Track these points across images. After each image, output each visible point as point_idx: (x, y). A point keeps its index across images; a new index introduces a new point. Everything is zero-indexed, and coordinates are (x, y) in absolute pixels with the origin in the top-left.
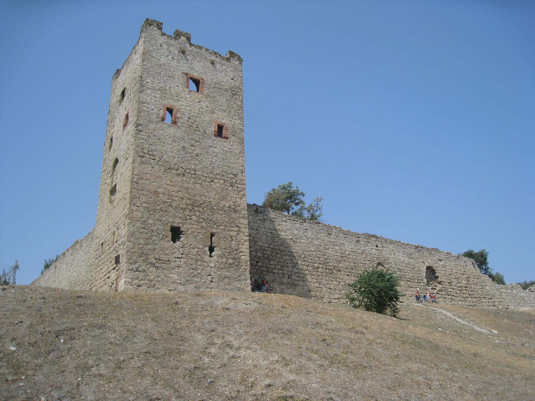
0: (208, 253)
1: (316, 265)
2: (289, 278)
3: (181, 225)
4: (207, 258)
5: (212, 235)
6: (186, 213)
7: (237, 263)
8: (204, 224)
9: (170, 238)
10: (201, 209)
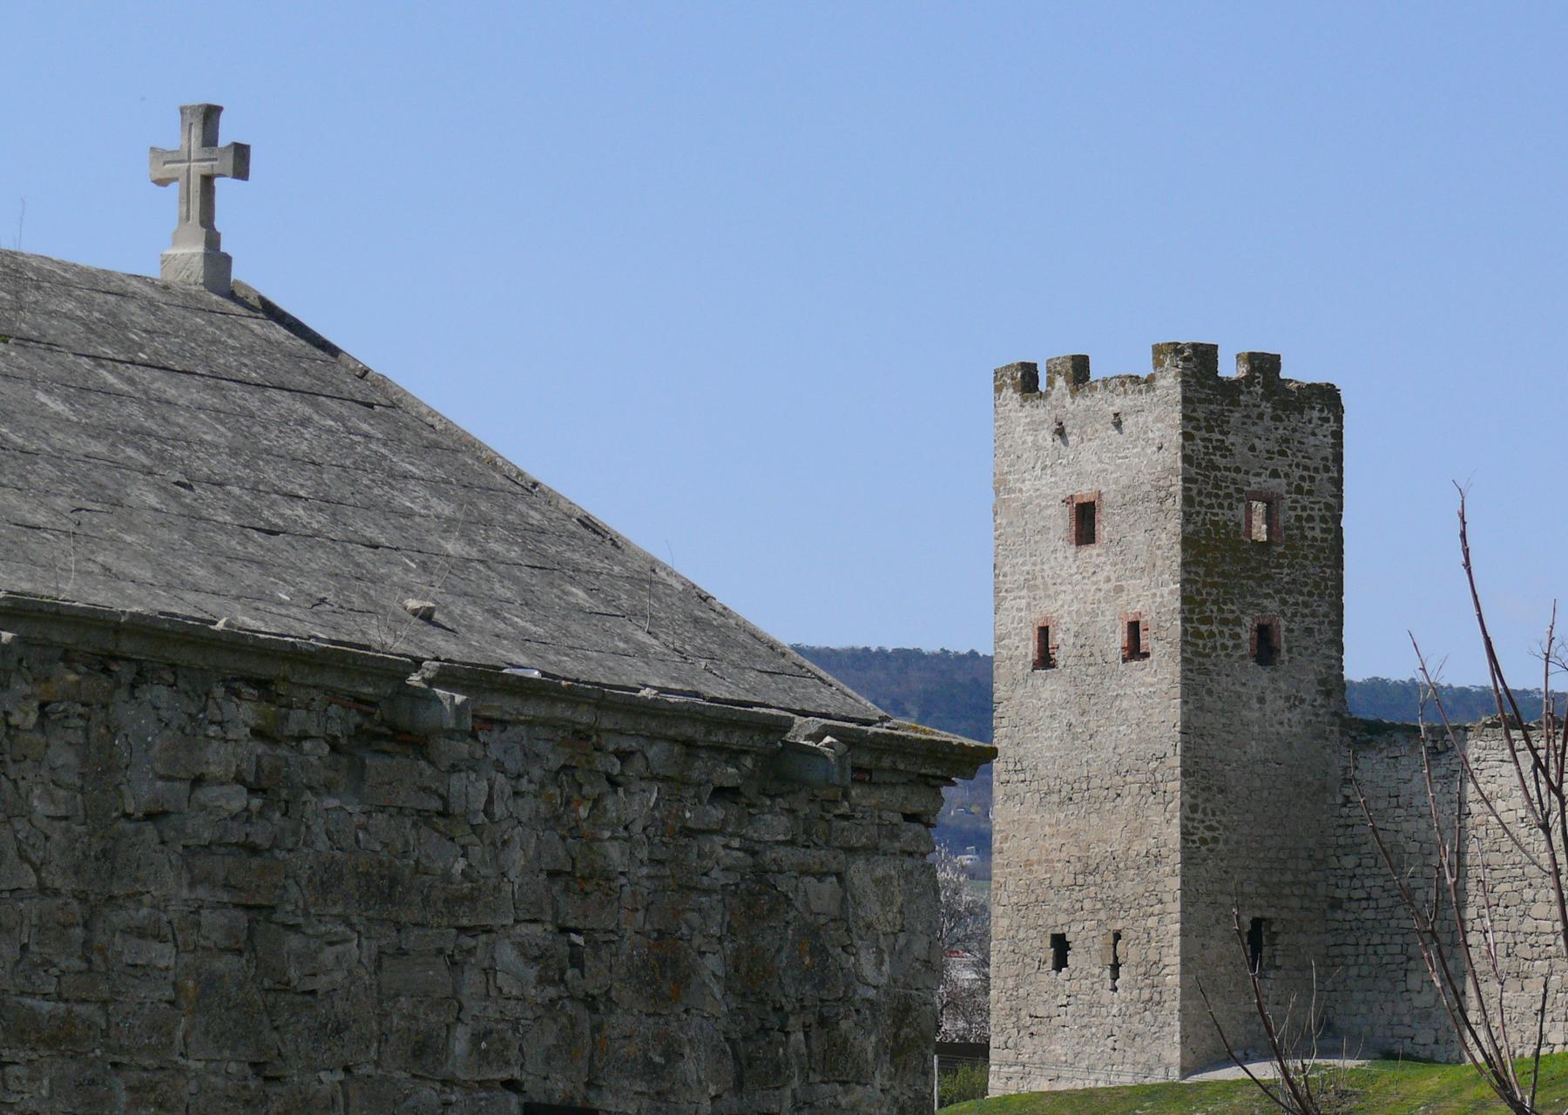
0: (1109, 984)
2: (1508, 955)
3: (1066, 929)
4: (1107, 995)
5: (1117, 936)
6: (1075, 895)
7: (1156, 997)
8: (1102, 915)
9: (1050, 962)
10: (1098, 879)
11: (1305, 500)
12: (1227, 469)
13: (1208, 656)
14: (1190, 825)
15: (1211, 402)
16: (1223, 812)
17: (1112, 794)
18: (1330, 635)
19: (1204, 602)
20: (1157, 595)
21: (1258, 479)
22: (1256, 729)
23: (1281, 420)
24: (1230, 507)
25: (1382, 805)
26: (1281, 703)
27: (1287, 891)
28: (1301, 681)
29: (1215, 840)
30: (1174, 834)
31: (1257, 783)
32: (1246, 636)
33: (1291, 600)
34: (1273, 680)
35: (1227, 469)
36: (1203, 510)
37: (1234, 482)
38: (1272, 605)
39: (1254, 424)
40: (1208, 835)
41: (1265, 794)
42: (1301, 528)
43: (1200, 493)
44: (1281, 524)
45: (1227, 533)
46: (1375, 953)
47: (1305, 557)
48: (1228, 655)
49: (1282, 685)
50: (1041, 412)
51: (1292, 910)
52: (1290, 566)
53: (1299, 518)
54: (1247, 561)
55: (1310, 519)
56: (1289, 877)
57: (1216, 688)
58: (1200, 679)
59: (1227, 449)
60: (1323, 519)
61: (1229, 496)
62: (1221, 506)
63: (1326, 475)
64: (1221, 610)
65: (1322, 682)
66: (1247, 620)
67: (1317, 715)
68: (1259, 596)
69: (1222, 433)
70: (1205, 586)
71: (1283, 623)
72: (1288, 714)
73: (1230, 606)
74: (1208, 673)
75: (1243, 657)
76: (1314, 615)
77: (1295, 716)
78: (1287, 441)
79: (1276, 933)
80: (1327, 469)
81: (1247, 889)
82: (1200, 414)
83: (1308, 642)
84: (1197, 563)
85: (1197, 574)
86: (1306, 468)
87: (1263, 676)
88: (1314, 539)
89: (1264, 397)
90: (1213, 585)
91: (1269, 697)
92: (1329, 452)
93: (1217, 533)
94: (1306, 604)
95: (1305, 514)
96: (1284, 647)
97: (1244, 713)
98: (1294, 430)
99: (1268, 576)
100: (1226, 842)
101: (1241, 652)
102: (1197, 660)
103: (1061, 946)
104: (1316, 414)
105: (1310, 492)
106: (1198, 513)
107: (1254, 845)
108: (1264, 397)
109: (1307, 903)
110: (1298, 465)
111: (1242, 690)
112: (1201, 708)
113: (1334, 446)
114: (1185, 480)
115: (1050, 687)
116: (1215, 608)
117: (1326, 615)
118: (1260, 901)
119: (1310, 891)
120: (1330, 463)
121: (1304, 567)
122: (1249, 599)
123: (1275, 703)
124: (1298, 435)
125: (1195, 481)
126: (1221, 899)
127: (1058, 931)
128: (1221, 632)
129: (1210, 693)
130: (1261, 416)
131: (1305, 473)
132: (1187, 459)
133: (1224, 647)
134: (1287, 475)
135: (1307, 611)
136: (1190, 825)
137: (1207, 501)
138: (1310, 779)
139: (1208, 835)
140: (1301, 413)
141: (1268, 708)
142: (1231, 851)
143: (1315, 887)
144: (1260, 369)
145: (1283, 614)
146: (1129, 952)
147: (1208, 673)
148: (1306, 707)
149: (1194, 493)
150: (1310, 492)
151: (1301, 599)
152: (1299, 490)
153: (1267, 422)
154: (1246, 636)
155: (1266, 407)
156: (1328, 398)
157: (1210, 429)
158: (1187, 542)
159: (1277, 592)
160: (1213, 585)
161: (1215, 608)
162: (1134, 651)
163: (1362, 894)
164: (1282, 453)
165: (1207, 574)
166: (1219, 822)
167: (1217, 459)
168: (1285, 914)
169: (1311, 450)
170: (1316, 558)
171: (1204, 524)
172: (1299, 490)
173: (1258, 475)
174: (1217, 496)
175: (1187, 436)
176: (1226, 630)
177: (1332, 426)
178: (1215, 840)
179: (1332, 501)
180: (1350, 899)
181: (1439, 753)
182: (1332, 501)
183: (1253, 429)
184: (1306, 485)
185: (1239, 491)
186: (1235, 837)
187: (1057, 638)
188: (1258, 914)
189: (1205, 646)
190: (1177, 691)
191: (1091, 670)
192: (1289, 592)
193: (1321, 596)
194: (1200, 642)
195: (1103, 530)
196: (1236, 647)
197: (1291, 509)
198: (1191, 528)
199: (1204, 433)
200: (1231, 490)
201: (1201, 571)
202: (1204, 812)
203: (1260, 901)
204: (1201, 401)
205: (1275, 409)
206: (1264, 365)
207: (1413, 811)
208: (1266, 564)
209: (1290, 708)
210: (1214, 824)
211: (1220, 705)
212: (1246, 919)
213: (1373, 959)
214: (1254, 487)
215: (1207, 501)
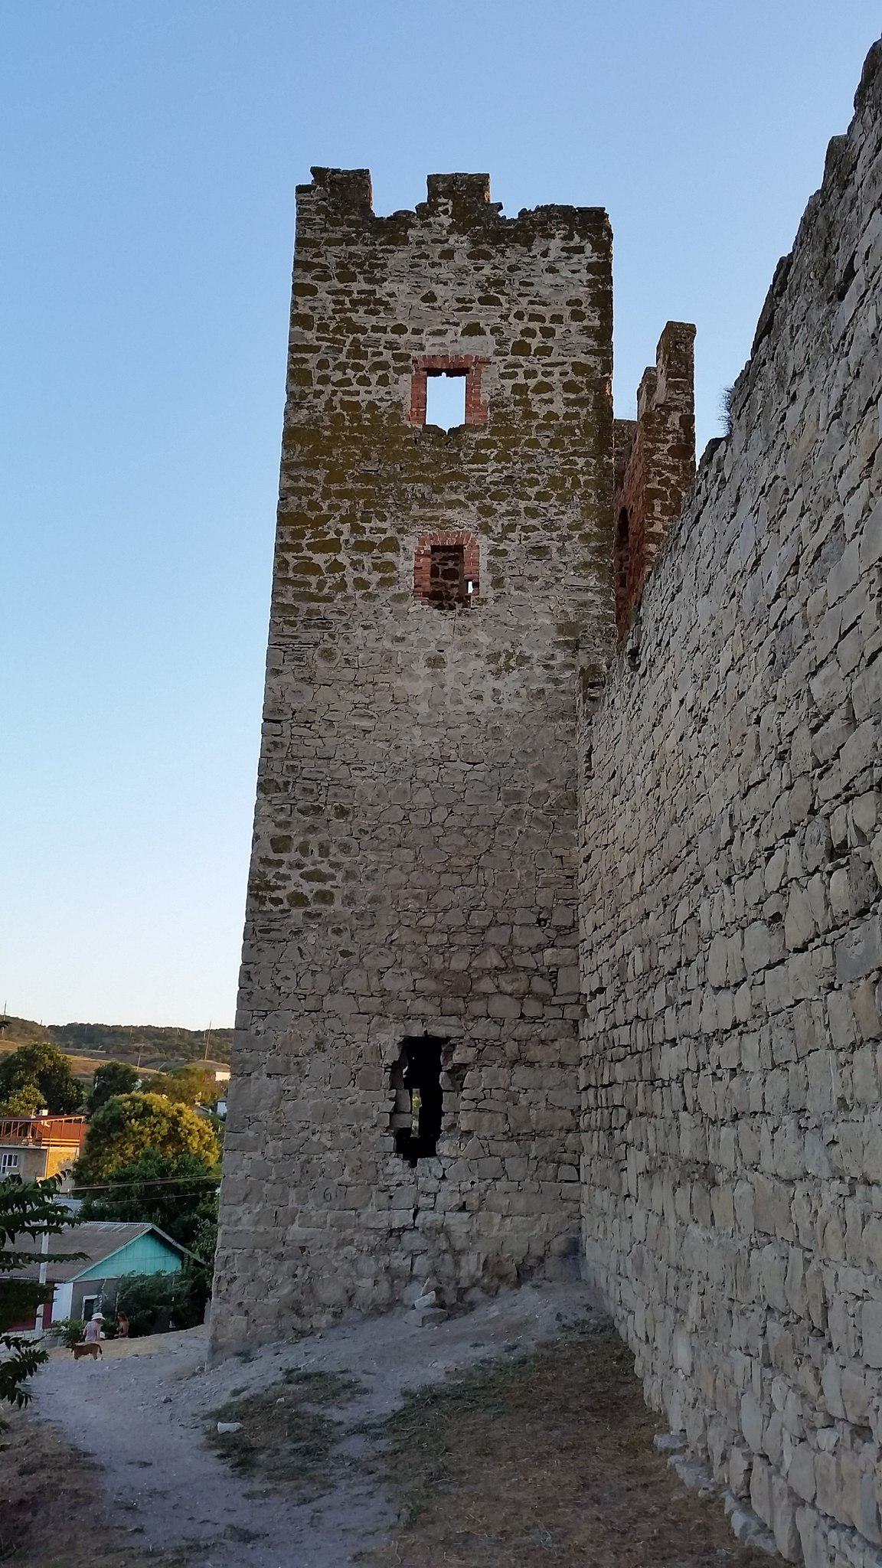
11: (535, 363)
12: (384, 330)
13: (328, 599)
14: (270, 873)
15: (350, 242)
16: (345, 848)
19: (328, 518)
21: (438, 340)
22: (423, 708)
23: (487, 256)
24: (383, 381)
26: (481, 663)
27: (486, 985)
28: (519, 628)
29: (325, 897)
31: (423, 797)
32: (405, 565)
34: (462, 630)
36: (330, 388)
37: (390, 346)
38: (464, 519)
39: (433, 265)
40: (308, 888)
41: (440, 814)
42: (527, 403)
43: (322, 364)
45: (376, 419)
48: (369, 597)
49: (483, 638)
51: (499, 1022)
52: (497, 459)
53: (517, 389)
54: (415, 456)
55: (548, 388)
56: (492, 960)
57: (341, 648)
58: (316, 634)
59: (379, 302)
60: (569, 387)
61: (384, 365)
62: (364, 381)
63: (575, 326)
64: (356, 529)
66: (410, 543)
67: (557, 682)
68: (440, 506)
69: (370, 281)
70: (326, 494)
72: (491, 683)
73: (376, 523)
74: (325, 624)
75: (399, 598)
76: (550, 526)
77: (510, 683)
78: (498, 283)
79: (463, 1066)
80: (577, 316)
81: (390, 983)
82: (331, 256)
83: (536, 568)
85: (309, 479)
86: (534, 317)
87: (440, 625)
88: (551, 415)
91: (451, 654)
92: (582, 293)
93: (359, 419)
94: (532, 513)
95: (532, 383)
96: (485, 578)
97: (399, 683)
98: (512, 269)
99: (455, 476)
100: (350, 900)
101: (394, 590)
102: (304, 606)
104: (555, 244)
105: (545, 351)
106: (318, 394)
107: (413, 905)
110: (519, 316)
111: (400, 647)
112: (309, 681)
113: (591, 284)
116: (346, 527)
117: (576, 526)
118: (420, 1006)
119: (540, 985)
122: (416, 510)
123: (466, 669)
125: (315, 350)
126: (328, 1003)
129: (328, 655)
130: (448, 255)
131: (536, 325)
133: (361, 584)
136: (270, 873)
137: (338, 376)
138: (541, 786)
139: (308, 888)
140: (528, 243)
141: (449, 674)
142: (360, 916)
143: (554, 976)
144: (449, 193)
145: (486, 529)
147: (325, 624)
149: (311, 365)
150: (545, 351)
151: (522, 504)
153: (460, 260)
154: (405, 565)
155: (460, 243)
158: (291, 436)
159: (472, 497)
160: (341, 495)
161: (346, 527)
166: (335, 865)
167: (359, 317)
168: (482, 1029)
169: (545, 292)
172: (521, 348)
174: (357, 368)
175: (299, 289)
176: (368, 564)
177: (590, 255)
178: (325, 897)
179: (590, 360)
182: (590, 360)
183: (436, 270)
184: (535, 343)
186: (371, 889)
188: (417, 1030)
189: (321, 585)
192: (498, 497)
193: (563, 499)
194: (313, 579)
197: (503, 376)
199: (336, 284)
201: (320, 475)
202: (304, 849)
203: (420, 1006)
204: (330, 242)
205: (475, 243)
206: (461, 196)
208: (454, 459)
209: (497, 674)
210: (325, 868)
211: (349, 674)
212: (389, 1040)
214: (429, 351)
215: (338, 376)
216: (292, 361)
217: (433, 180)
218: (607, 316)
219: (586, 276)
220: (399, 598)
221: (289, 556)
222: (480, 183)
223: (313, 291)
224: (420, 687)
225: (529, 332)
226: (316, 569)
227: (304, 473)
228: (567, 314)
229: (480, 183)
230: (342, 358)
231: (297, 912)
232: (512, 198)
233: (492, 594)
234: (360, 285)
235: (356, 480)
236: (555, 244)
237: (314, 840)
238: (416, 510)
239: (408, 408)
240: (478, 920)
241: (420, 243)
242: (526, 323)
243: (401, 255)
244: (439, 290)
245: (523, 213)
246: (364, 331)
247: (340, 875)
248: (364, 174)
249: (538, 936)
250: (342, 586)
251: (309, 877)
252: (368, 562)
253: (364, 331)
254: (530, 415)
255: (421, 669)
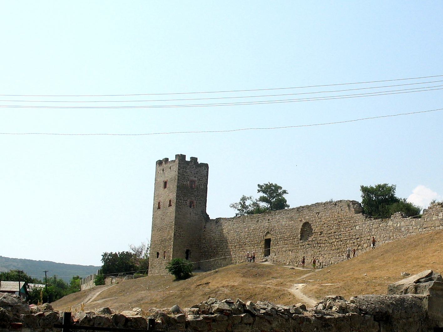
1: (235, 244)
9: (156, 257)
15: (184, 164)
17: (166, 229)
18: (204, 204)
20: (173, 196)
25: (209, 231)
26: (194, 214)
30: (173, 234)
33: (197, 198)
34: (193, 211)
35: (186, 175)
40: (179, 235)
44: (196, 185)
46: (207, 256)
47: (200, 191)
49: (194, 212)
50: (161, 168)
53: (199, 185)
55: (201, 185)
60: (204, 185)
61: (186, 180)
63: (205, 178)
64: (184, 198)
65: (202, 211)
66: (188, 200)
67: (201, 217)
70: (181, 194)
71: (195, 201)
75: (187, 206)
76: (201, 200)
77: (197, 217)
79: (191, 252)
80: (205, 177)
82: (182, 166)
84: (179, 190)
88: (202, 188)
89: (194, 164)
90: (183, 194)
91: (192, 213)
94: (200, 199)
96: (195, 205)
98: (199, 170)
101: (187, 205)
103: (158, 254)
104: (203, 168)
108: (194, 164)
109: (197, 248)
113: (206, 173)
114: (178, 177)
115: (159, 212)
120: (206, 176)
121: (200, 193)
124: (200, 171)
127: (158, 252)
128: (184, 202)
130: (193, 167)
131: (201, 177)
132: (178, 173)
134: (197, 177)
135: (200, 200)
136: (176, 233)
140: (201, 167)
146: (166, 254)
148: (199, 215)
150: (202, 181)
152: (200, 180)
154: (188, 203)
156: (206, 166)
157: (184, 169)
158: (178, 187)
159: (194, 196)
160: (183, 194)
162: (170, 205)
163: (205, 246)
164: (197, 174)
165: (182, 192)
170: (202, 191)
171: (181, 184)
172: (200, 180)
173: (192, 177)
176: (185, 202)
180: (204, 247)
181: (217, 222)
184: (201, 179)
185: (188, 179)
186: (184, 236)
187: (161, 204)
190: (175, 211)
191: (165, 209)
193: (203, 198)
194: (179, 203)
195: (168, 186)
196: (186, 204)
198: (179, 184)
200: (187, 179)
204: (182, 164)
205: (196, 166)
206: (194, 160)
207: (213, 232)
212: (185, 249)
213: (207, 257)
216: (178, 178)
217: (192, 158)
218: (208, 177)
219: (206, 172)
220: (187, 206)
221: (177, 200)
222: (197, 159)
223: (180, 170)
224: (189, 216)
225: (200, 178)
226: (180, 202)
227: (179, 191)
228: (204, 176)
229: (197, 159)
230: (183, 178)
231: (178, 237)
232: (199, 161)
233: (196, 207)
234: (184, 170)
235: (184, 192)
236: (203, 168)
237: (179, 230)
238: (189, 197)
239: (189, 185)
240: (193, 239)
241: (190, 165)
242: (200, 177)
243: (189, 167)
244: (192, 171)
245: (201, 163)
246: (185, 175)
247: (181, 234)
248: (185, 156)
249: (198, 241)
250: (182, 204)
251: (179, 234)
252: (185, 202)
253: (185, 175)
254: (200, 188)
255: (189, 214)
